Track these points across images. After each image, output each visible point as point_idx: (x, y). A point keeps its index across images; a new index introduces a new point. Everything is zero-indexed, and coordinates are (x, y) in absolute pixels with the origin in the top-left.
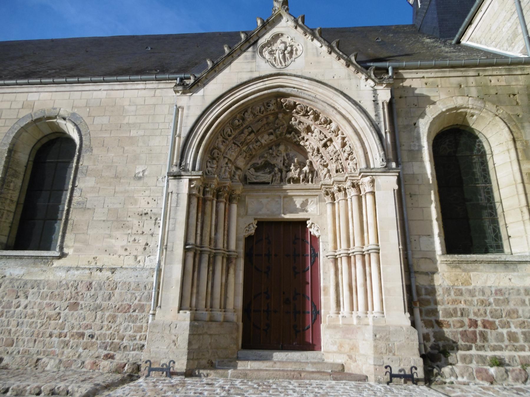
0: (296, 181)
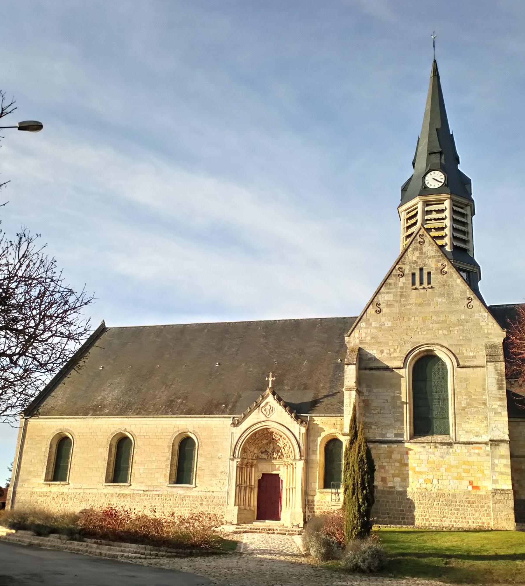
0: (276, 458)
